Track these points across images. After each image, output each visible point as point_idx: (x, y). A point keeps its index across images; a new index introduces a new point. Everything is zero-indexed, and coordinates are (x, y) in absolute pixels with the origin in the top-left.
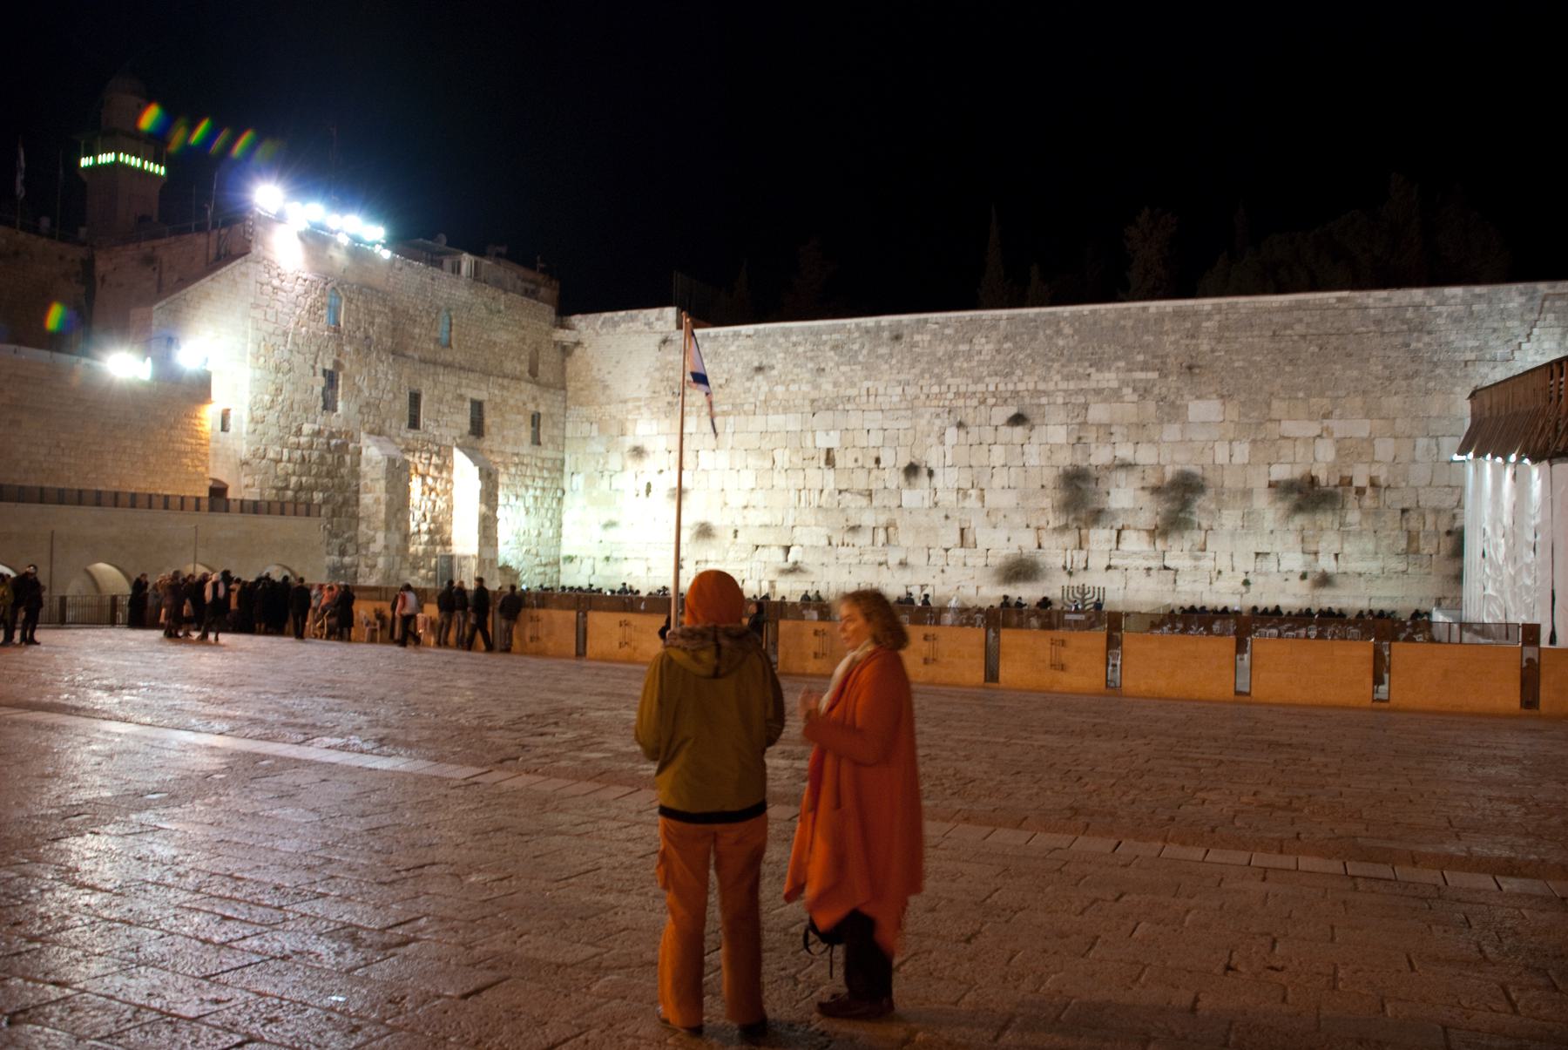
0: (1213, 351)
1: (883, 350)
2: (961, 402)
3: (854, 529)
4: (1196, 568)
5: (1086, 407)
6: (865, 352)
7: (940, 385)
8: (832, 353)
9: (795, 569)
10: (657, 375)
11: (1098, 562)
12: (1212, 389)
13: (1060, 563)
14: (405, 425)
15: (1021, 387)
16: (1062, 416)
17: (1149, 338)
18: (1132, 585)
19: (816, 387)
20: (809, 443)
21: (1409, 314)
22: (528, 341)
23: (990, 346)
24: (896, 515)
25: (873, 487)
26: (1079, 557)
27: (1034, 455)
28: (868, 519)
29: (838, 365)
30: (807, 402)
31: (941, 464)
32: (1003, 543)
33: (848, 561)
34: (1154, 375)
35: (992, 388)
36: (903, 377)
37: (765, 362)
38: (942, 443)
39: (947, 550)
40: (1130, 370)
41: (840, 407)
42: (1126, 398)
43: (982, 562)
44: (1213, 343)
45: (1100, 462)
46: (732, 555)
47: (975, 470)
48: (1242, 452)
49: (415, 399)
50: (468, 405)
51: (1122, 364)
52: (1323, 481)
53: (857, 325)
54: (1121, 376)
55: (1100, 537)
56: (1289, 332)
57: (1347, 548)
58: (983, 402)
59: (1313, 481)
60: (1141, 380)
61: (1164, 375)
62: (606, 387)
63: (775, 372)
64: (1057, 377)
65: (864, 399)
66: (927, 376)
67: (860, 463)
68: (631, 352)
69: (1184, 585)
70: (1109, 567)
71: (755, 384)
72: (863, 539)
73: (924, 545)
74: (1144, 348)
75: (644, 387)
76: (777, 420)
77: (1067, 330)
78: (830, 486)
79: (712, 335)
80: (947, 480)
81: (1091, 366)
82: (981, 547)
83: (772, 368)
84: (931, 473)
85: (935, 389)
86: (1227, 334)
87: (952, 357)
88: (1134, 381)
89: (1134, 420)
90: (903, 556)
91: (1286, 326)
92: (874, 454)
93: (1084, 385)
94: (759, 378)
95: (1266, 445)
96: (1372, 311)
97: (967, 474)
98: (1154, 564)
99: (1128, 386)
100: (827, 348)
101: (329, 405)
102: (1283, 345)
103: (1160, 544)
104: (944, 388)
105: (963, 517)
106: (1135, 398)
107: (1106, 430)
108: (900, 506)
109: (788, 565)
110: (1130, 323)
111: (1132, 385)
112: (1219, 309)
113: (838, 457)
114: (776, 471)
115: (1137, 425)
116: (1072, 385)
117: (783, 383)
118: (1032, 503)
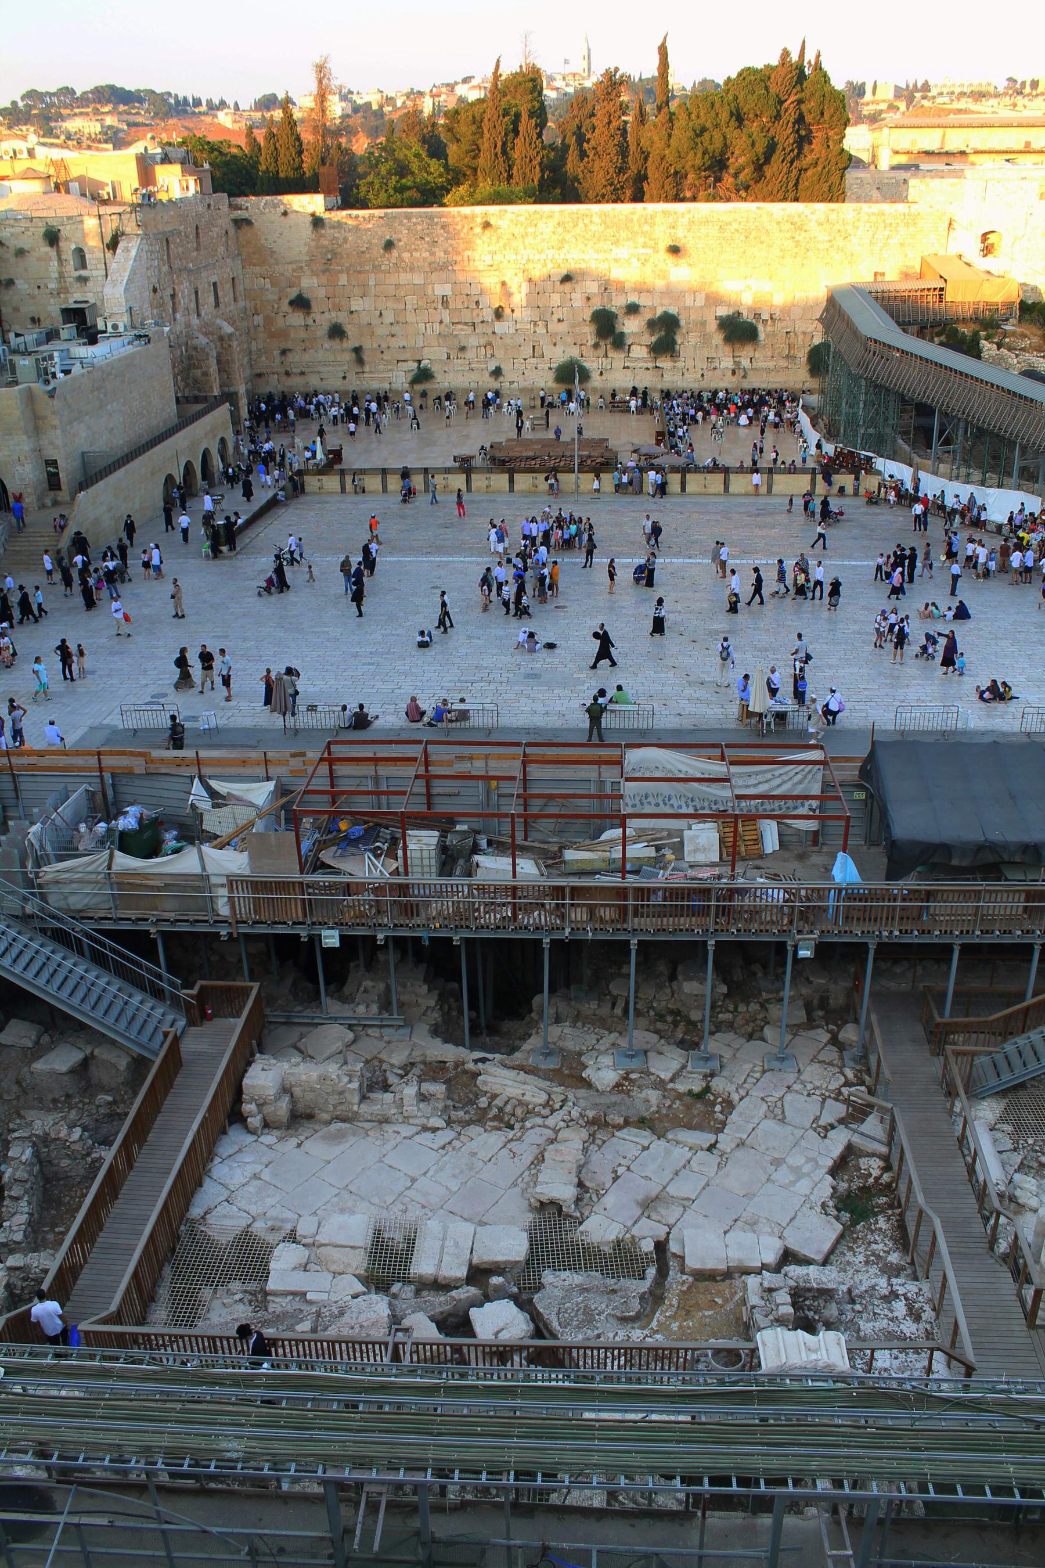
1: (478, 230)
3: (463, 349)
10: (313, 244)
15: (569, 257)
18: (638, 378)
19: (433, 254)
20: (430, 292)
21: (796, 219)
24: (492, 339)
25: (477, 320)
27: (578, 301)
28: (473, 341)
29: (447, 239)
32: (560, 355)
34: (650, 251)
36: (492, 248)
51: (631, 243)
52: (745, 314)
57: (757, 355)
61: (656, 251)
69: (667, 377)
72: (470, 354)
74: (644, 234)
76: (404, 278)
77: (596, 219)
82: (546, 358)
83: (400, 240)
85: (513, 257)
87: (524, 236)
97: (537, 312)
98: (650, 365)
110: (635, 218)
118: (577, 330)
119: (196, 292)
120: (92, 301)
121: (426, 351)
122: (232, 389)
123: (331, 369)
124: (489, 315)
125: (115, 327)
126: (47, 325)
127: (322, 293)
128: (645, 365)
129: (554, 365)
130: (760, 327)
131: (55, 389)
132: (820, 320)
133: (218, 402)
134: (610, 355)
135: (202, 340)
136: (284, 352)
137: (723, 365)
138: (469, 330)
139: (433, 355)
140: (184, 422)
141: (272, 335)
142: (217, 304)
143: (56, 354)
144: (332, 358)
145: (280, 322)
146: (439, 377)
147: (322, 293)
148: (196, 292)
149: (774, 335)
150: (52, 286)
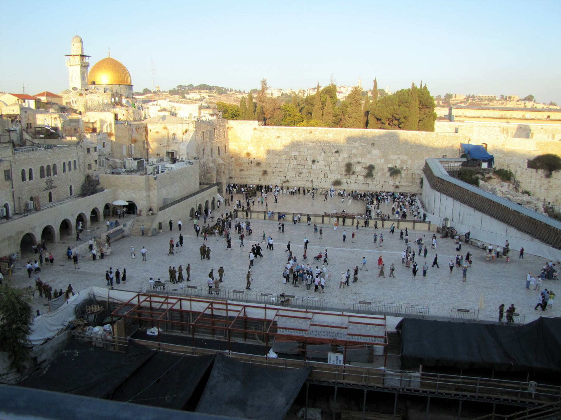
2: (325, 147)
3: (300, 173)
5: (351, 150)
9: (287, 181)
11: (353, 182)
18: (360, 186)
20: (291, 154)
24: (310, 170)
26: (349, 181)
27: (340, 159)
28: (304, 171)
32: (334, 177)
34: (366, 144)
37: (280, 135)
43: (329, 181)
48: (382, 161)
52: (398, 167)
55: (353, 177)
57: (402, 181)
58: (330, 147)
59: (396, 167)
62: (240, 138)
69: (370, 186)
72: (303, 175)
80: (322, 163)
82: (329, 178)
84: (318, 162)
91: (392, 137)
92: (306, 157)
93: (351, 145)
94: (279, 139)
95: (387, 161)
103: (365, 179)
107: (355, 156)
109: (286, 180)
116: (349, 145)
119: (212, 149)
120: (177, 150)
121: (288, 173)
122: (221, 181)
124: (310, 162)
125: (182, 159)
126: (161, 156)
130: (403, 172)
131: (156, 177)
132: (423, 170)
133: (214, 185)
134: (350, 178)
135: (212, 165)
136: (241, 170)
137: (390, 184)
138: (303, 167)
139: (291, 175)
140: (201, 191)
141: (237, 165)
142: (219, 154)
143: (160, 166)
148: (212, 149)
149: (407, 174)
150: (165, 144)
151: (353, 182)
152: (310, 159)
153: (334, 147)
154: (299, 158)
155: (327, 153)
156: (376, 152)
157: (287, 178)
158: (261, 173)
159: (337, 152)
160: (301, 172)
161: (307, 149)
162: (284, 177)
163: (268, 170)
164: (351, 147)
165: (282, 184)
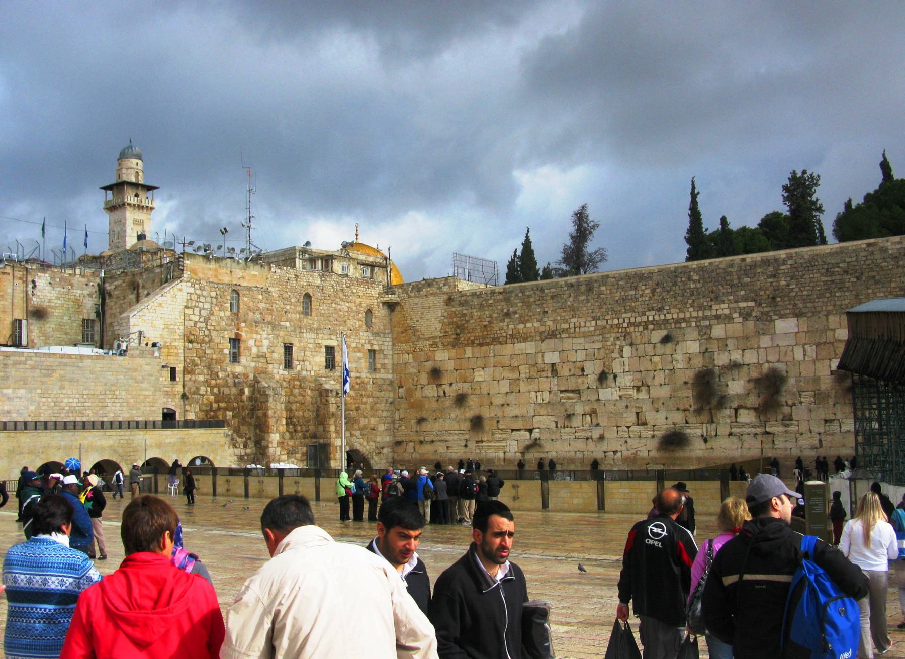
0: (788, 285)
1: (582, 298)
2: (632, 329)
4: (786, 432)
5: (710, 327)
6: (571, 299)
7: (618, 319)
8: (551, 301)
11: (724, 430)
12: (788, 311)
13: (699, 432)
14: (281, 367)
15: (669, 316)
16: (695, 335)
17: (747, 280)
18: (746, 445)
20: (540, 361)
22: (363, 305)
23: (648, 291)
24: (595, 406)
25: (581, 388)
30: (538, 334)
31: (622, 370)
33: (569, 437)
34: (753, 304)
35: (651, 318)
37: (511, 309)
38: (622, 357)
39: (628, 427)
40: (736, 302)
41: (558, 336)
42: (735, 320)
44: (788, 279)
45: (721, 364)
46: (497, 436)
47: (644, 373)
49: (288, 349)
50: (324, 350)
53: (566, 282)
54: (732, 305)
56: (836, 269)
58: (646, 328)
60: (744, 307)
63: (517, 316)
64: (691, 309)
65: (572, 330)
66: (610, 313)
67: (572, 373)
68: (430, 308)
69: (780, 444)
70: (730, 434)
71: (506, 323)
72: (576, 422)
73: (614, 424)
75: (439, 329)
76: (520, 347)
77: (696, 277)
78: (555, 388)
79: (478, 293)
81: (712, 300)
83: (515, 313)
84: (615, 377)
86: (797, 273)
88: (740, 308)
89: (741, 335)
90: (602, 432)
93: (708, 313)
96: (890, 252)
97: (638, 376)
99: (735, 312)
100: (549, 298)
101: (235, 358)
102: (833, 278)
104: (621, 320)
105: (637, 405)
106: (741, 320)
107: (723, 343)
108: (598, 400)
111: (738, 310)
112: (790, 257)
113: (559, 368)
114: (521, 382)
115: (743, 338)
116: (701, 314)
117: (523, 323)
118: (679, 394)
121: (536, 419)
123: (456, 437)
124: (592, 380)
127: (451, 365)
128: (753, 430)
129: (659, 433)
134: (715, 420)
136: (421, 421)
144: (456, 427)
145: (418, 394)
146: (547, 446)
147: (451, 365)
148: (288, 349)
151: (724, 430)
152: (593, 369)
153: (657, 325)
154: (564, 371)
155: (641, 347)
156: (785, 326)
157: (536, 434)
158: (466, 425)
159: (666, 340)
160: (570, 412)
161: (582, 340)
162: (528, 434)
163: (486, 413)
164: (705, 318)
165: (523, 453)
